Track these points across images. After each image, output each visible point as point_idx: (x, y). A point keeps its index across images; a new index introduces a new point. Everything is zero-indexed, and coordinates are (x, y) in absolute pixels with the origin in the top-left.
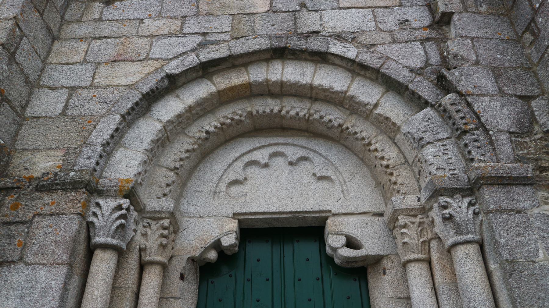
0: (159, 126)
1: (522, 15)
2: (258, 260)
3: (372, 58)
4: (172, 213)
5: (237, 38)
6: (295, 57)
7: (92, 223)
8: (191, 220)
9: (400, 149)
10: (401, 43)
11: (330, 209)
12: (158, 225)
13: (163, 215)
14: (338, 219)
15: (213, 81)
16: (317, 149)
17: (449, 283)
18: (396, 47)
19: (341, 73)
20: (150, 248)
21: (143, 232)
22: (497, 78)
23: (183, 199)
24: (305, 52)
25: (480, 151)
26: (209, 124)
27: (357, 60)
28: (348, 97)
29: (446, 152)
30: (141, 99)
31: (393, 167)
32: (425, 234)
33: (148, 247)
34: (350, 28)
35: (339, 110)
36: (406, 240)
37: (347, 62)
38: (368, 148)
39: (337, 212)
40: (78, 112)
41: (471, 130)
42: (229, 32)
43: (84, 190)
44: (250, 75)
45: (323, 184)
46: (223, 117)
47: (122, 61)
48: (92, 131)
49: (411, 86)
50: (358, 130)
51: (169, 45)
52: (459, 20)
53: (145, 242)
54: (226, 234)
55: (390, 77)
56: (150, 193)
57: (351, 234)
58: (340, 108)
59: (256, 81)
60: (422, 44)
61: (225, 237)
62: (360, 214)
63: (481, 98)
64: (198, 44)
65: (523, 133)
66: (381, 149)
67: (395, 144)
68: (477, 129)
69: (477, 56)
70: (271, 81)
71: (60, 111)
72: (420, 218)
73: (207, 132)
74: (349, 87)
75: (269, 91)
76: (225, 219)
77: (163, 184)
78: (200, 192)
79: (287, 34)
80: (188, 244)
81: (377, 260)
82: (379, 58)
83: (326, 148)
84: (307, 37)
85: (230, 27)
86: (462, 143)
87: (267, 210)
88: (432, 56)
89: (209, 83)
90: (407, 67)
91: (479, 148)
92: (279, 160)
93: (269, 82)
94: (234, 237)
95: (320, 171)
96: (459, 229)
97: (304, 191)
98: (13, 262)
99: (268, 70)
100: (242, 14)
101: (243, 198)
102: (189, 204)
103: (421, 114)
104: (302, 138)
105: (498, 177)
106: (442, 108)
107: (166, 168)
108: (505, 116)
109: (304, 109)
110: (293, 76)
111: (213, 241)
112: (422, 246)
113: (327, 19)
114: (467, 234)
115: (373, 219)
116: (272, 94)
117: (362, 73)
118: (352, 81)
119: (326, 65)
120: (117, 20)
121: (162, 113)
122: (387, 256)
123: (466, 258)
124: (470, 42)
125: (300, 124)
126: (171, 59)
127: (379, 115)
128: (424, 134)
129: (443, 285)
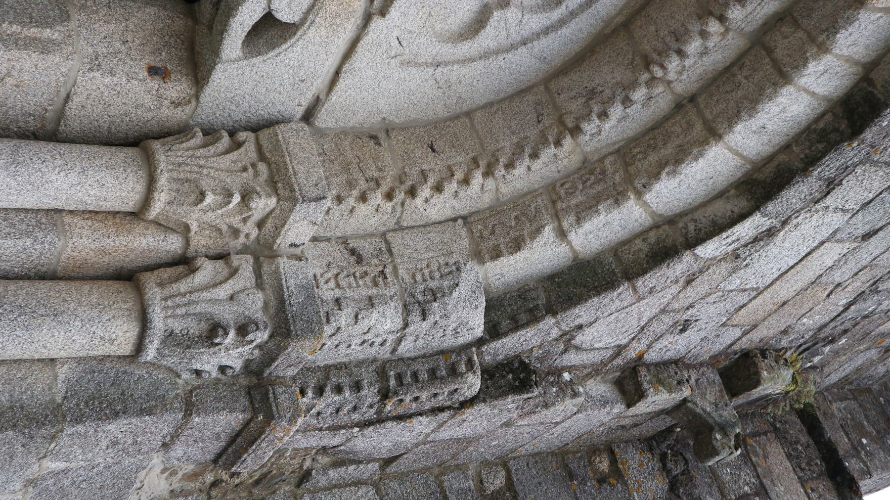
1: (540, 483)
6: (815, 130)
11: (387, 16)
17: (60, 254)
24: (801, 166)
31: (403, 204)
32: (207, 232)
35: (614, 144)
36: (210, 199)
37: (700, 230)
38: (483, 164)
41: (383, 406)
49: (550, 321)
50: (537, 165)
55: (598, 294)
57: (292, 41)
58: (617, 147)
59: (849, 21)
62: (337, 73)
70: (816, 57)
75: (796, 24)
86: (367, 376)
91: (338, 411)
93: (815, 49)
95: (502, 23)
96: (178, 344)
105: (256, 440)
106: (463, 368)
109: (680, 73)
116: (781, 19)
117: (652, 236)
119: (732, 180)
122: (197, 97)
125: (652, 28)
127: (538, 231)
129: (59, 245)
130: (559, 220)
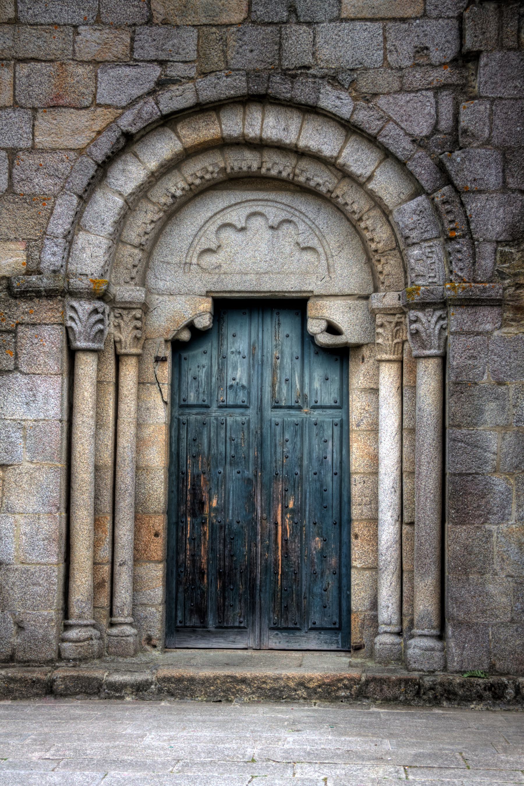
0: (120, 201)
2: (234, 336)
3: (371, 118)
4: (144, 303)
5: (205, 74)
7: (71, 327)
8: (161, 298)
9: (393, 230)
10: (410, 92)
12: (130, 316)
13: (134, 306)
14: (321, 302)
15: (178, 133)
16: (303, 210)
18: (403, 98)
19: (333, 129)
20: (125, 341)
21: (116, 324)
22: (506, 161)
23: (149, 271)
25: (461, 264)
26: (176, 185)
27: (352, 121)
28: (339, 164)
29: (430, 255)
30: (96, 171)
33: (123, 340)
34: (350, 62)
35: (330, 170)
39: (319, 294)
40: (26, 188)
42: (194, 61)
43: (60, 297)
44: (223, 126)
45: (308, 256)
46: (192, 175)
47: (63, 106)
48: (49, 218)
50: (349, 201)
51: (119, 79)
52: (486, 65)
53: (119, 335)
54: (200, 315)
56: (116, 277)
58: (331, 168)
59: (230, 136)
60: (435, 96)
61: (198, 318)
62: (343, 296)
63: (479, 196)
64: (155, 82)
65: (513, 240)
66: (371, 229)
67: (389, 222)
68: (463, 236)
69: (491, 131)
71: (5, 187)
72: (398, 318)
73: (174, 196)
74: (340, 151)
76: (198, 299)
77: (129, 266)
78: (168, 263)
79: (269, 69)
80: (160, 326)
81: (358, 347)
82: (379, 120)
83: (313, 208)
84: (294, 76)
85: (196, 52)
87: (243, 289)
88: (444, 117)
89: (173, 135)
90: (410, 135)
92: (257, 223)
94: (208, 318)
97: (285, 264)
98: (9, 371)
99: (244, 119)
100: (210, 25)
101: (217, 271)
102: (157, 278)
103: (413, 204)
104: (286, 193)
107: (130, 245)
108: (499, 221)
109: (288, 166)
110: (274, 131)
111: (186, 323)
112: (395, 347)
113: (322, 41)
114: (430, 349)
115: (357, 302)
118: (346, 142)
120: (42, 25)
121: (120, 183)
122: (367, 344)
123: (425, 371)
124: (488, 106)
126: (123, 108)
127: (372, 190)
128: (411, 232)
130: (364, 183)
